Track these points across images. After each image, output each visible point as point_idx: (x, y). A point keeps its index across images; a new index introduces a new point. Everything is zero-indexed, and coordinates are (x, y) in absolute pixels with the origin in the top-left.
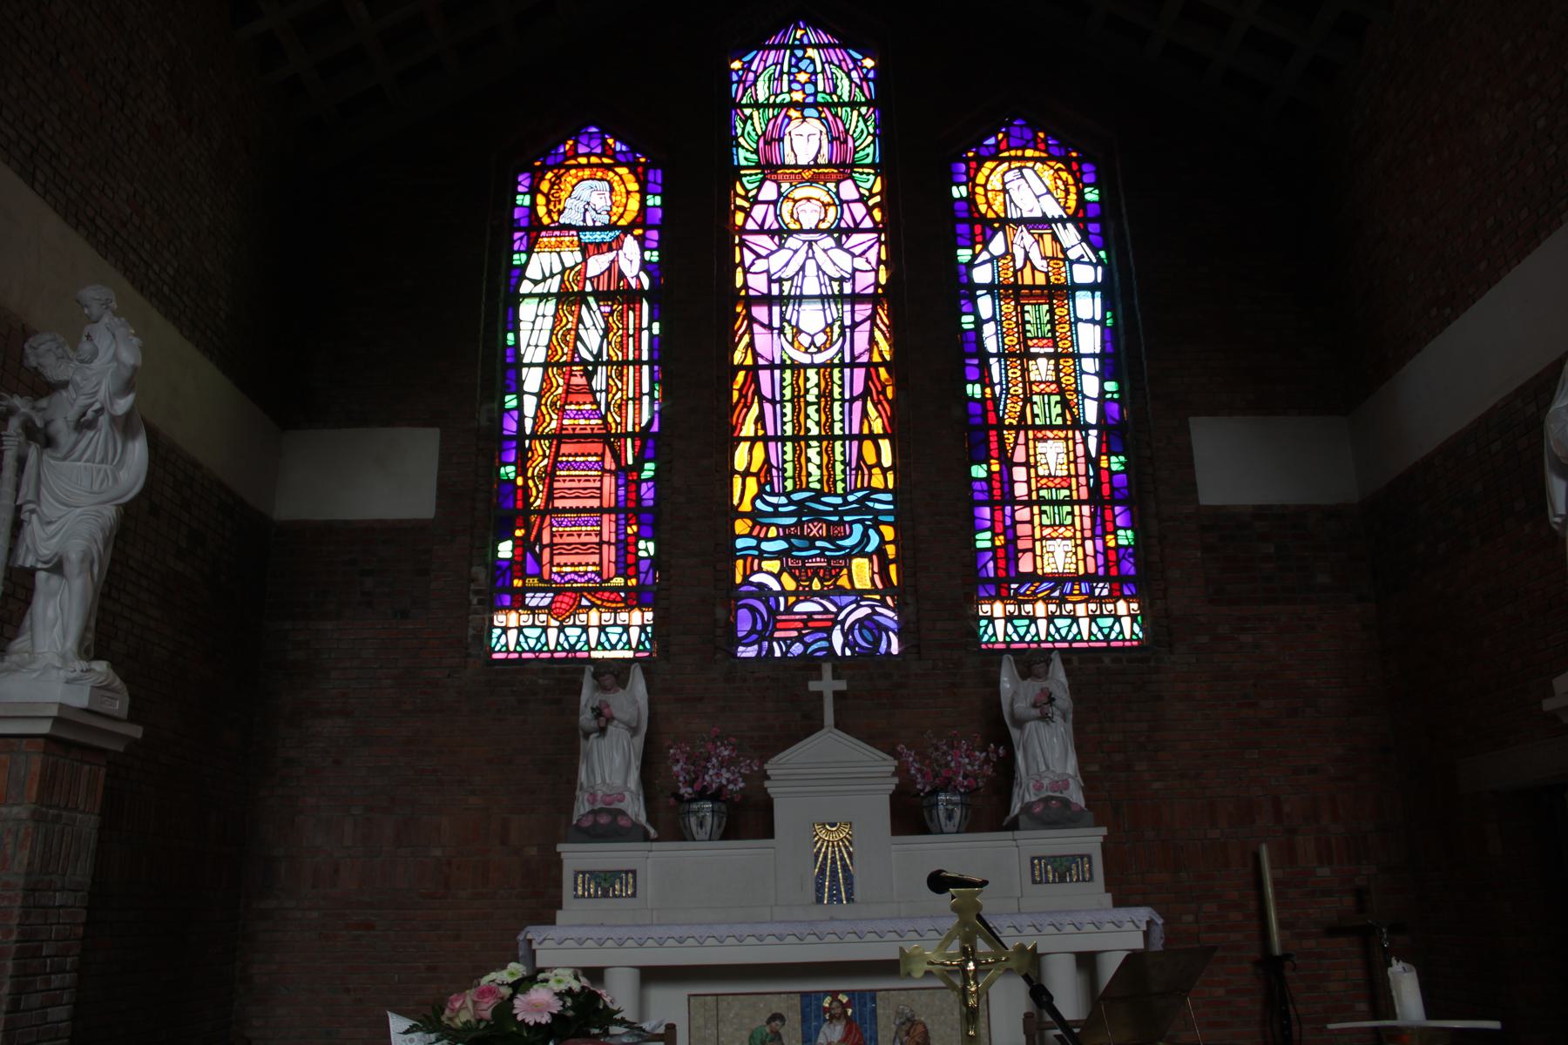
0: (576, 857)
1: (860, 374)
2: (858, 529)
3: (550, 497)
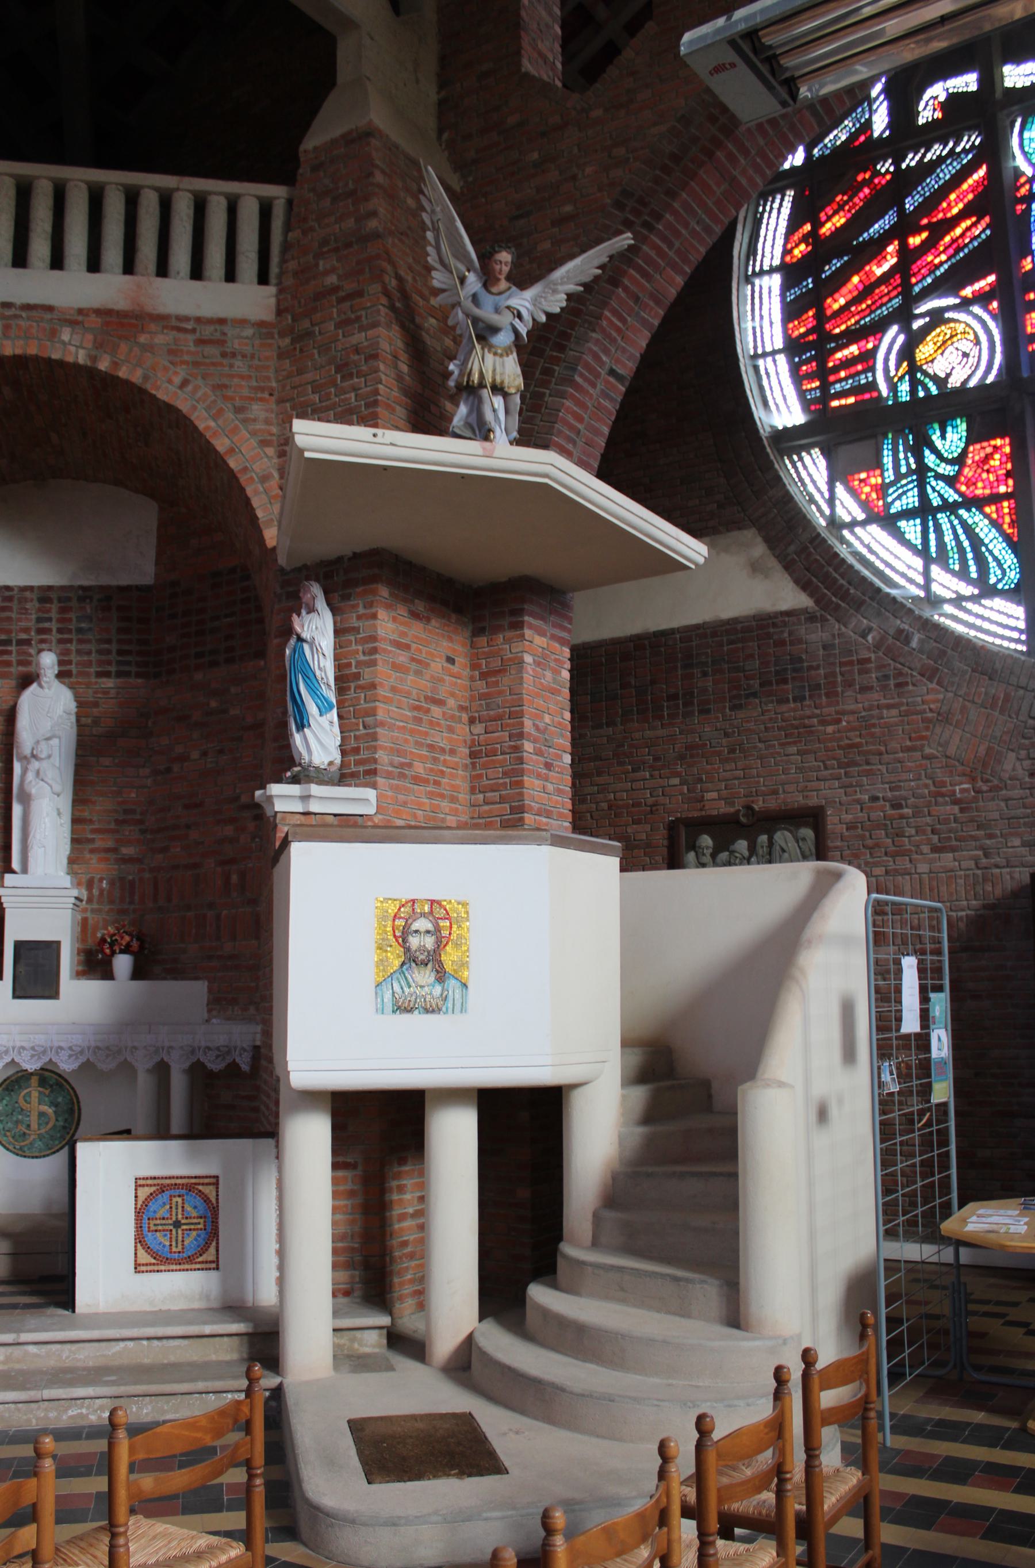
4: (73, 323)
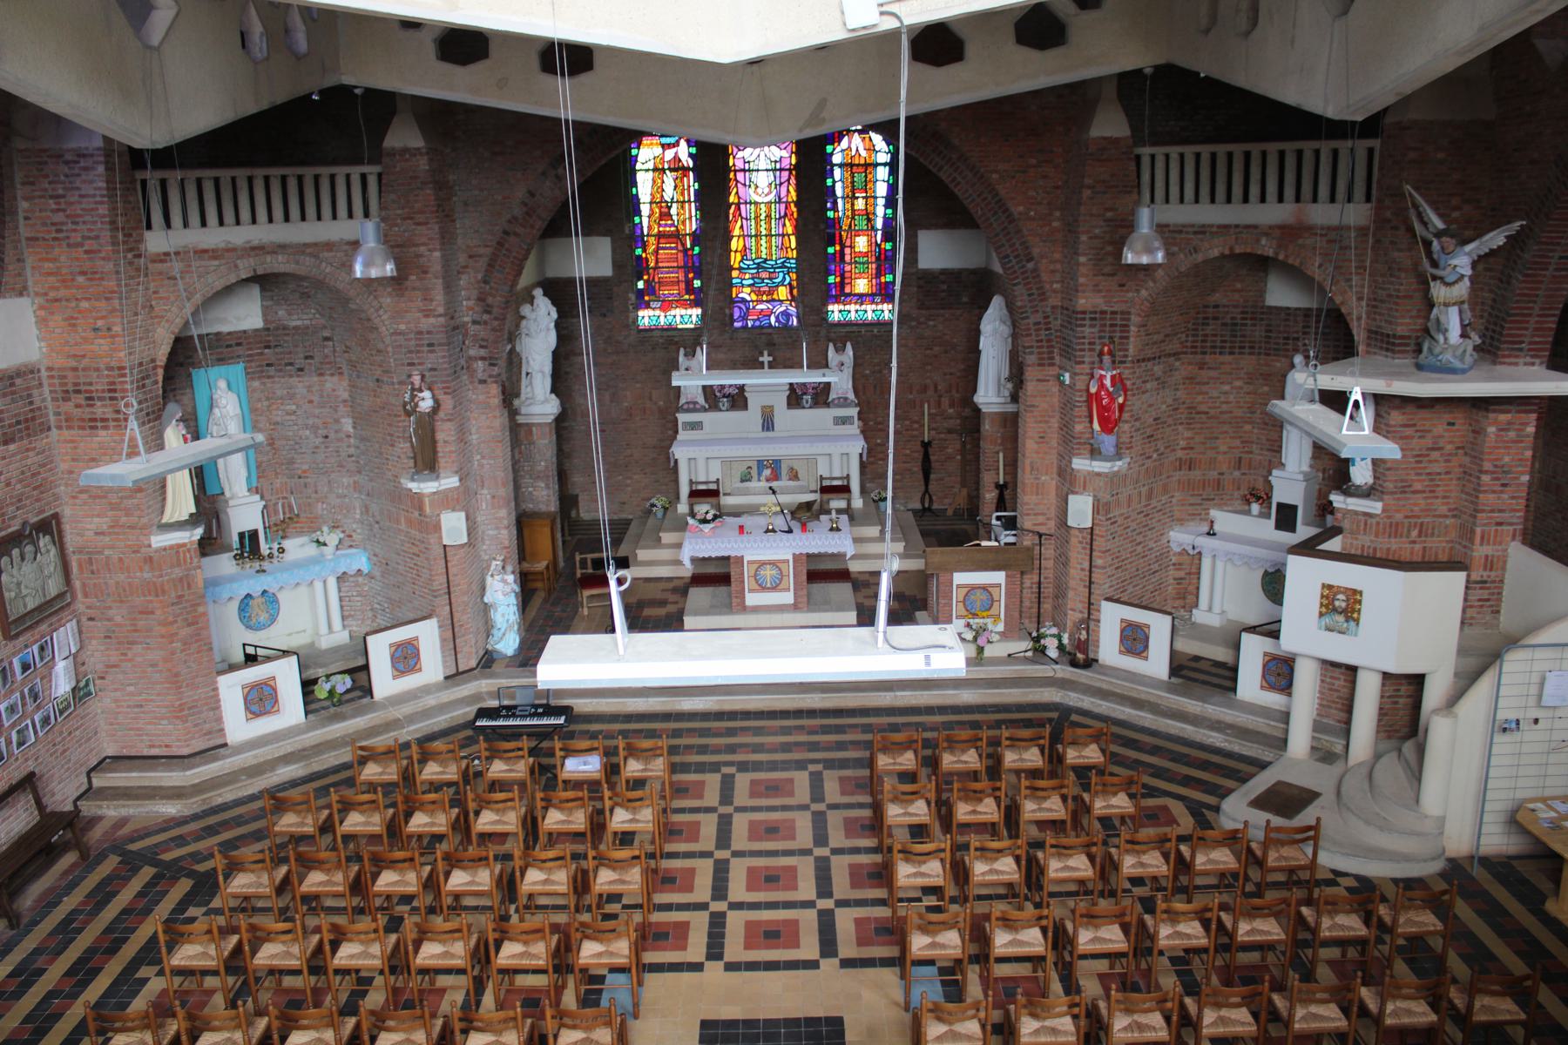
0: (682, 418)
3: (657, 262)
4: (1267, 234)
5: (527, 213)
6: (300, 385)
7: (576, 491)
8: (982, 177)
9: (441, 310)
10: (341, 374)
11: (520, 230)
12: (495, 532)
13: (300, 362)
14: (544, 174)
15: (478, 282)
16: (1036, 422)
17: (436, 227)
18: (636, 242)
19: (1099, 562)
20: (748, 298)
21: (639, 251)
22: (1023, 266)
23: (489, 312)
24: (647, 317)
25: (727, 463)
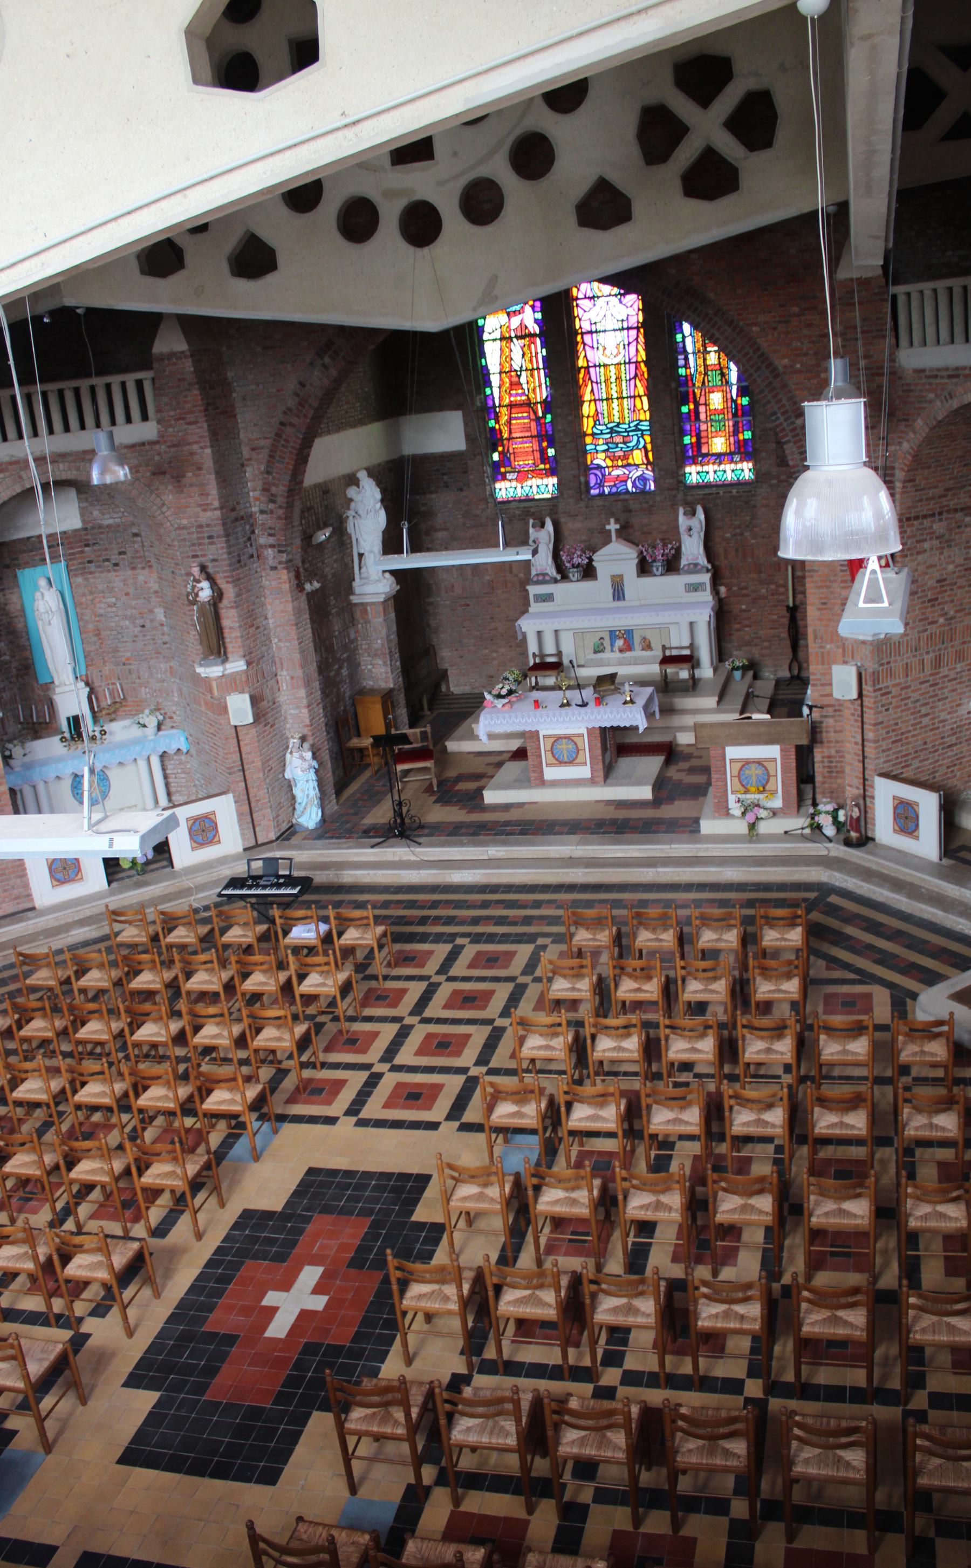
0: (533, 590)
1: (633, 366)
2: (635, 438)
3: (510, 433)
5: (300, 404)
6: (117, 579)
7: (446, 666)
8: (741, 330)
9: (216, 504)
10: (150, 567)
11: (295, 420)
12: (296, 712)
13: (115, 558)
14: (311, 364)
15: (262, 473)
16: (817, 587)
17: (205, 425)
18: (489, 414)
19: (870, 735)
20: (604, 465)
21: (492, 423)
22: (793, 423)
23: (274, 502)
24: (505, 489)
25: (579, 634)
